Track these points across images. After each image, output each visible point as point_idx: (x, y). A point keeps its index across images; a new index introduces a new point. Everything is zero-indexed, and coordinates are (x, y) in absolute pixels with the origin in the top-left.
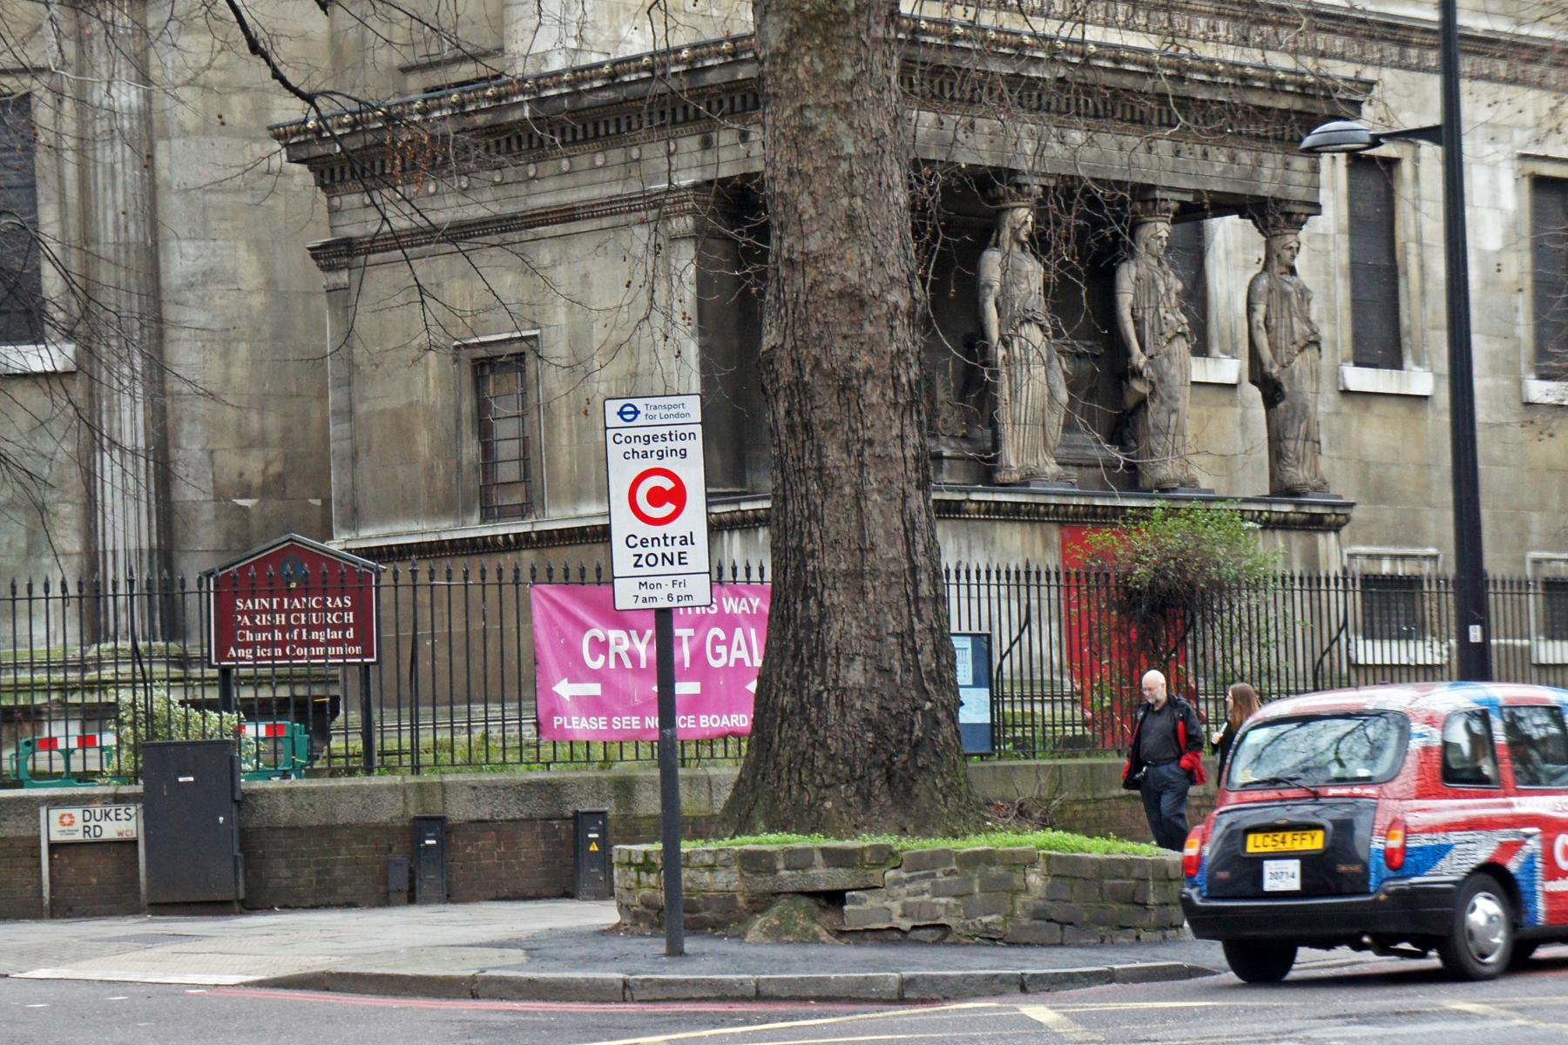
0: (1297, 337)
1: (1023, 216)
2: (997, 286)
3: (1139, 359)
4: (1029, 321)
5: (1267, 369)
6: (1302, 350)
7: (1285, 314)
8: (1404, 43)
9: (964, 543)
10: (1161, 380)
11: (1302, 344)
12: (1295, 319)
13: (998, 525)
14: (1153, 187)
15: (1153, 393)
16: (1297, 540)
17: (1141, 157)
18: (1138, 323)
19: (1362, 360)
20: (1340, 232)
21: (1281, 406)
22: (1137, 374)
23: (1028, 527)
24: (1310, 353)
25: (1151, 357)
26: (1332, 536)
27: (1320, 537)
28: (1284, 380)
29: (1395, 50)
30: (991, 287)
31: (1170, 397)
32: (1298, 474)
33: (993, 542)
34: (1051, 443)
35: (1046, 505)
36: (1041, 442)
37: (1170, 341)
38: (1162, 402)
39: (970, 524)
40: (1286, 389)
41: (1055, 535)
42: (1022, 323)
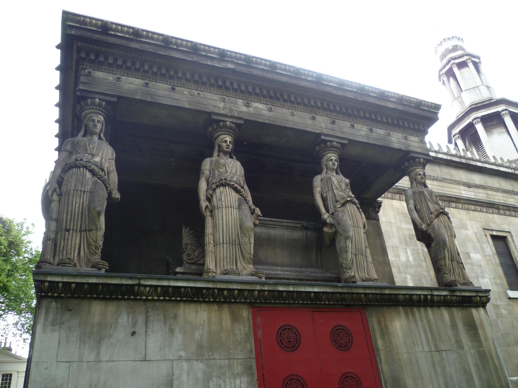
0: (432, 210)
1: (226, 140)
2: (207, 173)
3: (326, 216)
4: (223, 185)
5: (419, 227)
6: (437, 216)
7: (423, 201)
8: (498, 209)
9: (141, 319)
10: (339, 224)
11: (436, 213)
12: (429, 203)
13: (182, 305)
14: (319, 135)
15: (336, 233)
16: (458, 314)
17: (310, 122)
18: (324, 200)
19: (512, 289)
20: (493, 254)
21: (433, 245)
22: (325, 223)
23: (216, 307)
24: (443, 218)
25: (333, 214)
26: (481, 310)
27: (474, 311)
28: (429, 231)
29: (496, 211)
30: (203, 173)
31: (344, 231)
32: (449, 278)
33: (175, 317)
34: (247, 255)
35: (229, 290)
36: (239, 254)
37: (343, 205)
38: (341, 236)
39: (149, 304)
40: (433, 235)
41: (245, 313)
42: (218, 186)
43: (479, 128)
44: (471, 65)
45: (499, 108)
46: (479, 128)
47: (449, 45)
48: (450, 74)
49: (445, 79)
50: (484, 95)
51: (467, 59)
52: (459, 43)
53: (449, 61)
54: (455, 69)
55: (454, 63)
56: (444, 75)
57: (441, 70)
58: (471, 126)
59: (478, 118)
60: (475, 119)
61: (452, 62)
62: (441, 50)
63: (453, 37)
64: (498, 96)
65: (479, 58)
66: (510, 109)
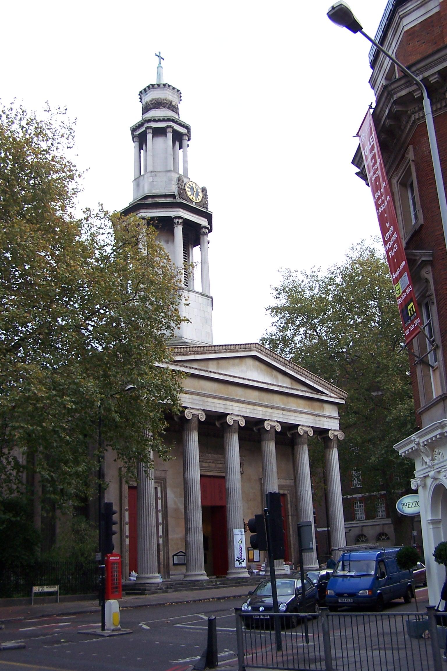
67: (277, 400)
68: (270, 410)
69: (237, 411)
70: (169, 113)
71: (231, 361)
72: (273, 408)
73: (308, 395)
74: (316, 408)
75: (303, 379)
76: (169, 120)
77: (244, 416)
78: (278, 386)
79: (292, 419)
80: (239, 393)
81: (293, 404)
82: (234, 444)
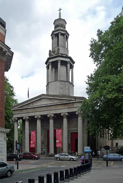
43: (59, 64)
44: (65, 36)
45: (68, 60)
46: (59, 64)
47: (61, 22)
48: (57, 35)
49: (54, 37)
50: (66, 53)
51: (65, 34)
52: (64, 24)
53: (59, 30)
54: (60, 35)
55: (60, 32)
56: (54, 35)
57: (53, 32)
58: (56, 62)
59: (60, 60)
60: (59, 60)
61: (60, 31)
62: (57, 23)
63: (64, 20)
64: (69, 55)
65: (68, 35)
66: (71, 62)
67: (53, 108)
68: (50, 111)
69: (37, 114)
70: (62, 28)
71: (37, 102)
72: (51, 110)
73: (67, 102)
74: (71, 106)
75: (62, 99)
76: (59, 30)
77: (40, 115)
78: (50, 104)
79: (58, 112)
80: (39, 109)
81: (59, 107)
82: (39, 123)
